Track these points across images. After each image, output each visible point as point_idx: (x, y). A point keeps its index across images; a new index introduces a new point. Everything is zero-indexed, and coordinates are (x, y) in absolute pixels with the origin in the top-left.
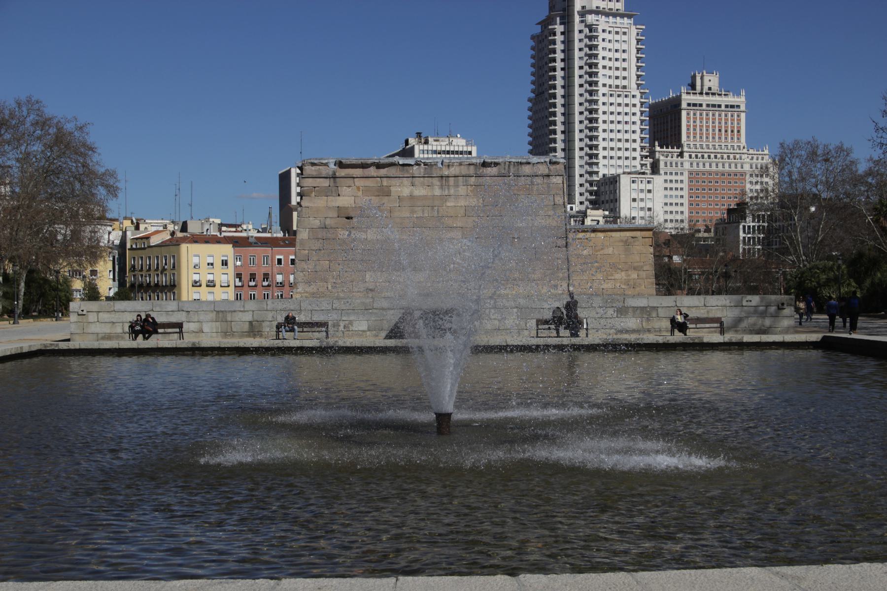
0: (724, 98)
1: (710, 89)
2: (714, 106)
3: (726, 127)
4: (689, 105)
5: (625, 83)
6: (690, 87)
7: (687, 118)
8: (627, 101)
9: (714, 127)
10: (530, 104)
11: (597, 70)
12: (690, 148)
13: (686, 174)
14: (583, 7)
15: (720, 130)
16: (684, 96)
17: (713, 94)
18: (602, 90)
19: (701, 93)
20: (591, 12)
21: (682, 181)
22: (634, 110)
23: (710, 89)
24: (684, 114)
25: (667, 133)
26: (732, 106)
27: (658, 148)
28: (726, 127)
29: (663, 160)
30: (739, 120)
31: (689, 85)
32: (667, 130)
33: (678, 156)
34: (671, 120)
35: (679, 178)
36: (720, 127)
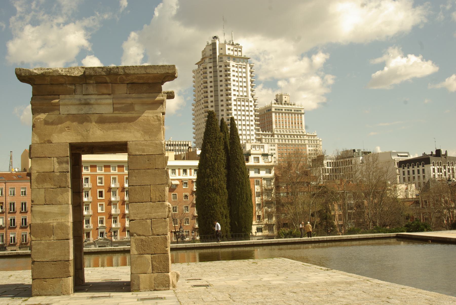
0: (293, 107)
1: (286, 102)
2: (288, 110)
3: (295, 121)
4: (276, 109)
5: (245, 94)
6: (275, 101)
7: (275, 116)
8: (247, 104)
9: (289, 121)
10: (193, 107)
11: (230, 87)
12: (277, 132)
13: (276, 145)
14: (221, 54)
15: (292, 123)
16: (273, 105)
17: (288, 104)
18: (233, 98)
19: (282, 104)
20: (226, 55)
21: (274, 149)
22: (251, 109)
23: (286, 102)
24: (273, 115)
25: (265, 125)
26: (297, 111)
27: (261, 132)
28: (295, 121)
29: (264, 138)
30: (301, 118)
31: (275, 100)
32: (265, 123)
33: (271, 137)
34: (267, 118)
35: (273, 148)
36: (292, 121)
